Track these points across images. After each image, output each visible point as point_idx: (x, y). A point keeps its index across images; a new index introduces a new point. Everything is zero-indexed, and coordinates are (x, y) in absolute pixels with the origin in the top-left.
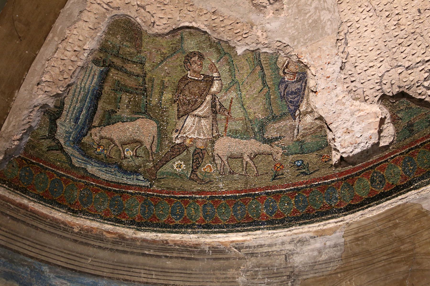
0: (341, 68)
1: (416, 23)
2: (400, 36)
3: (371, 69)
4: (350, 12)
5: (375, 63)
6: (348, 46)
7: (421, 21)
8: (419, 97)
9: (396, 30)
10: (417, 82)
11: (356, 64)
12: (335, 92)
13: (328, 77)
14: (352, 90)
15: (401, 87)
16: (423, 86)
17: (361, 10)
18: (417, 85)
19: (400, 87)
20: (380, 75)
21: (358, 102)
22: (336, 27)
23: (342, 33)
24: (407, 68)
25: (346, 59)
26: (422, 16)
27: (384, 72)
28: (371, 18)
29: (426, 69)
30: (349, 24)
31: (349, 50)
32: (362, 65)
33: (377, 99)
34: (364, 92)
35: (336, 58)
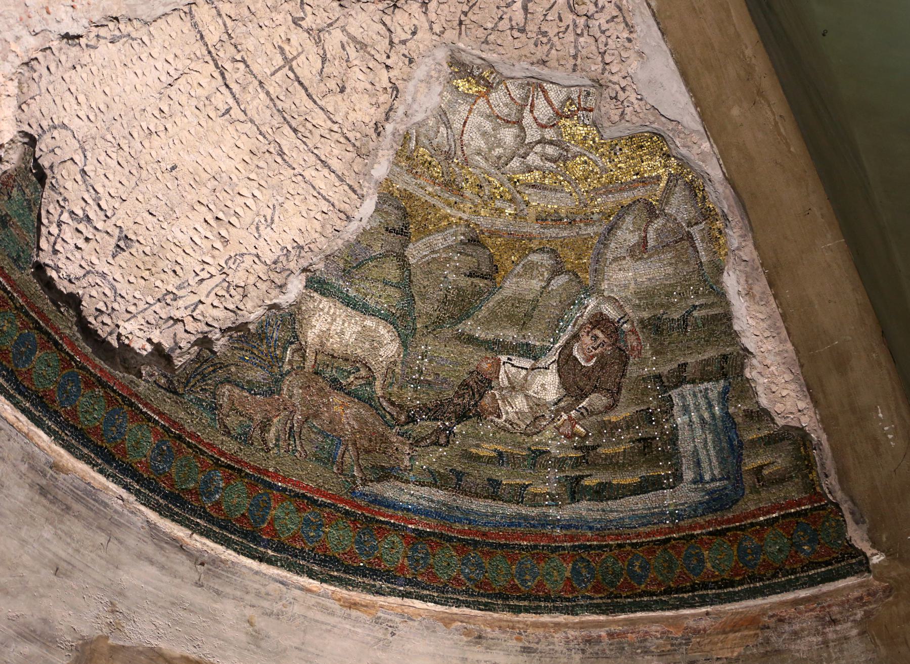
0: (67, 36)
1: (156, 166)
2: (133, 143)
3: (74, 101)
4: (168, 37)
5: (85, 107)
6: (109, 44)
7: (159, 175)
8: (43, 213)
9: (141, 133)
10: (65, 200)
11: (78, 67)
12: (24, 33)
13: (48, 13)
14: (35, 71)
15: (52, 171)
16: (62, 212)
17: (170, 58)
18: (60, 199)
19: (51, 167)
20: (66, 122)
21: (16, 91)
22: (139, 13)
23: (130, 29)
24: (85, 173)
25: (87, 46)
26: (167, 175)
27: (72, 127)
28: (157, 81)
29: (87, 208)
30: (146, 39)
31: (104, 47)
32: (78, 81)
33: (26, 128)
34: (33, 98)
35: (85, 22)
